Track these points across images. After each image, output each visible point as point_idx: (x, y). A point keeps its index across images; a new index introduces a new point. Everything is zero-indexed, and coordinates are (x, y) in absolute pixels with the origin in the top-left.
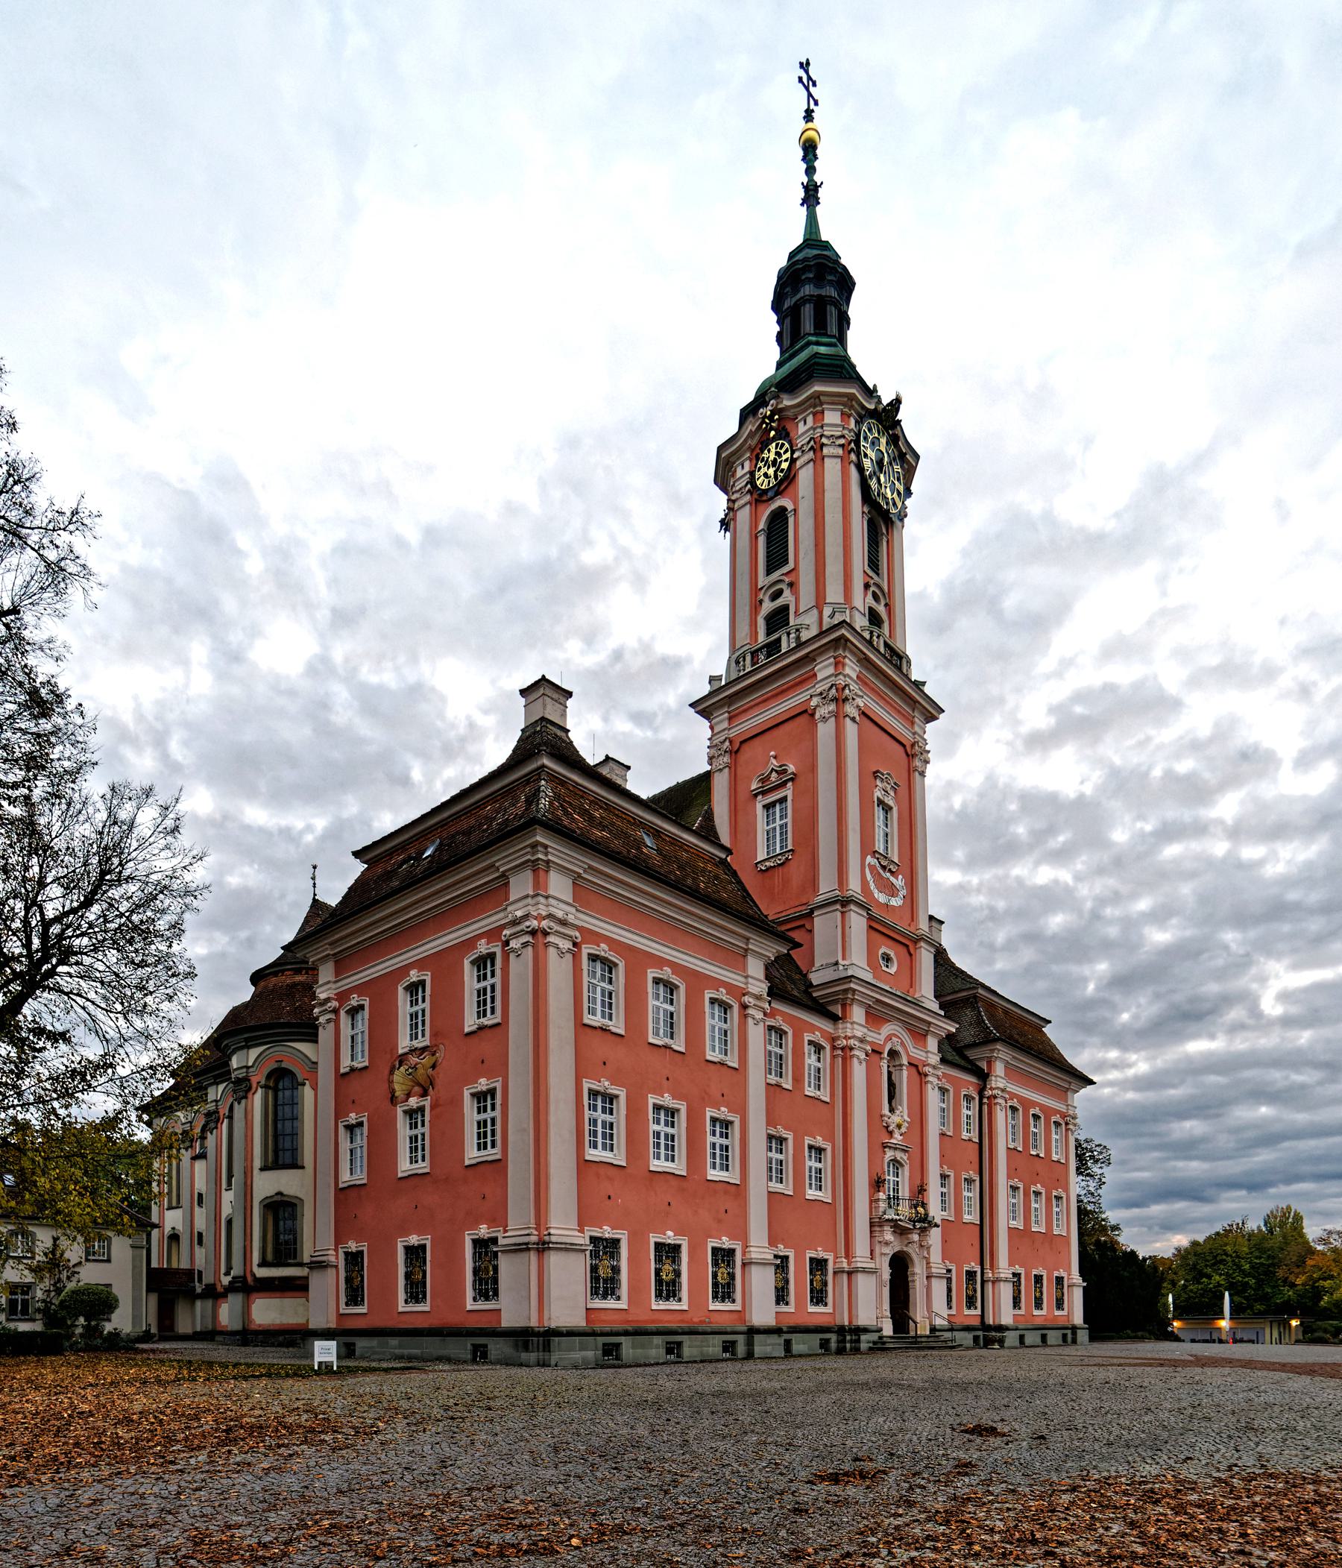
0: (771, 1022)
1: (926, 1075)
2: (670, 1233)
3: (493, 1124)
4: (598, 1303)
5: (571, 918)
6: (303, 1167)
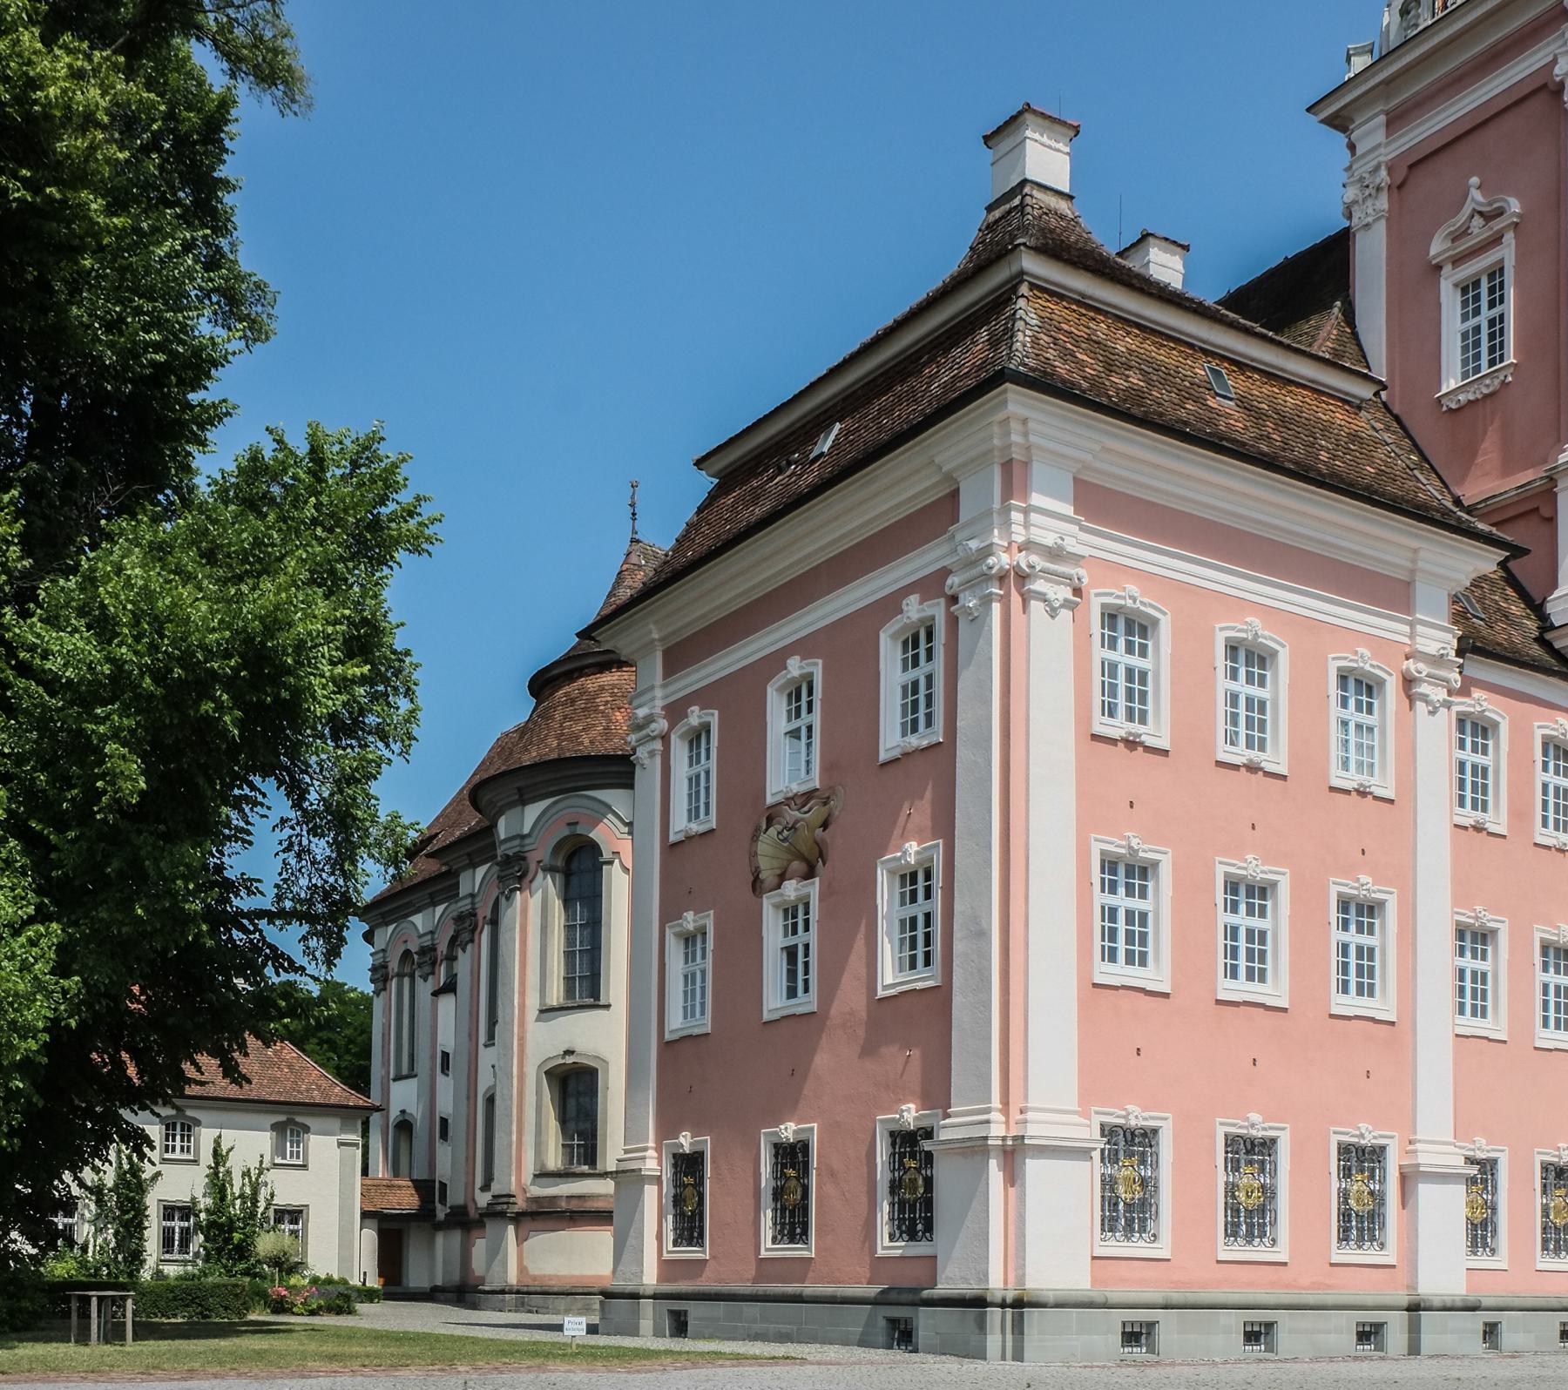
0: (1462, 705)
2: (1255, 1117)
3: (928, 923)
4: (1117, 1246)
5: (1071, 546)
6: (607, 1007)
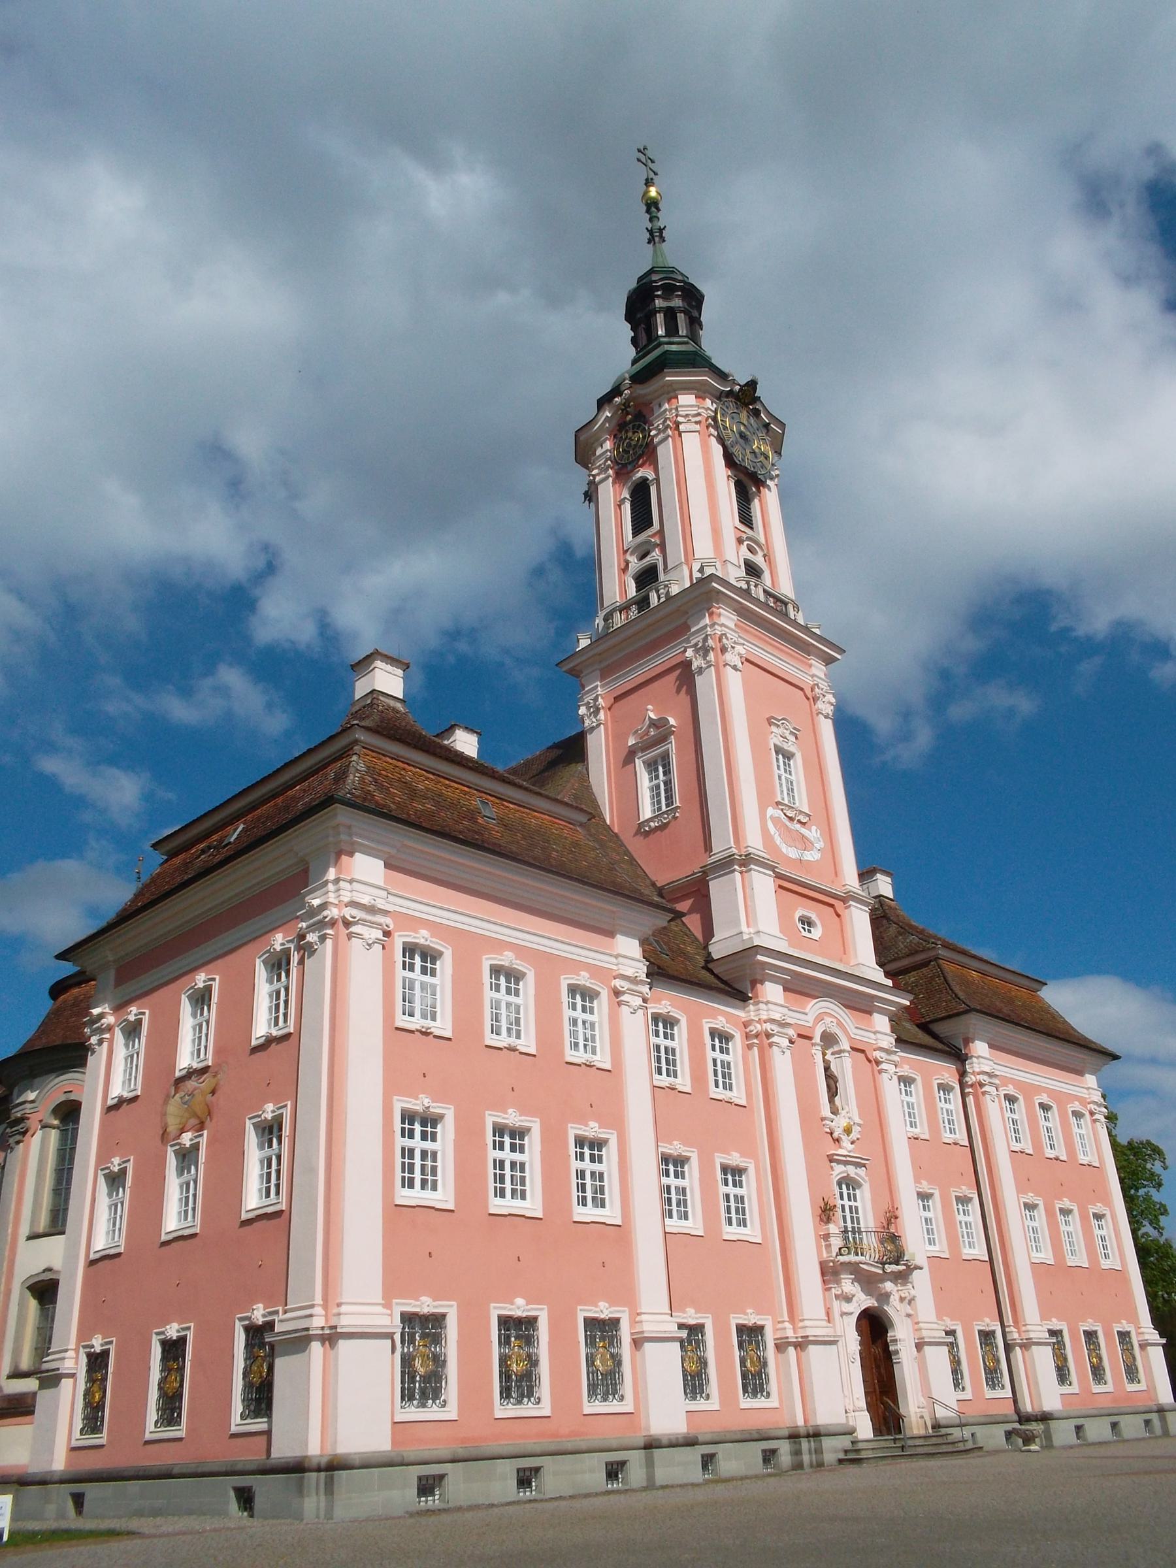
1: (878, 1063)
